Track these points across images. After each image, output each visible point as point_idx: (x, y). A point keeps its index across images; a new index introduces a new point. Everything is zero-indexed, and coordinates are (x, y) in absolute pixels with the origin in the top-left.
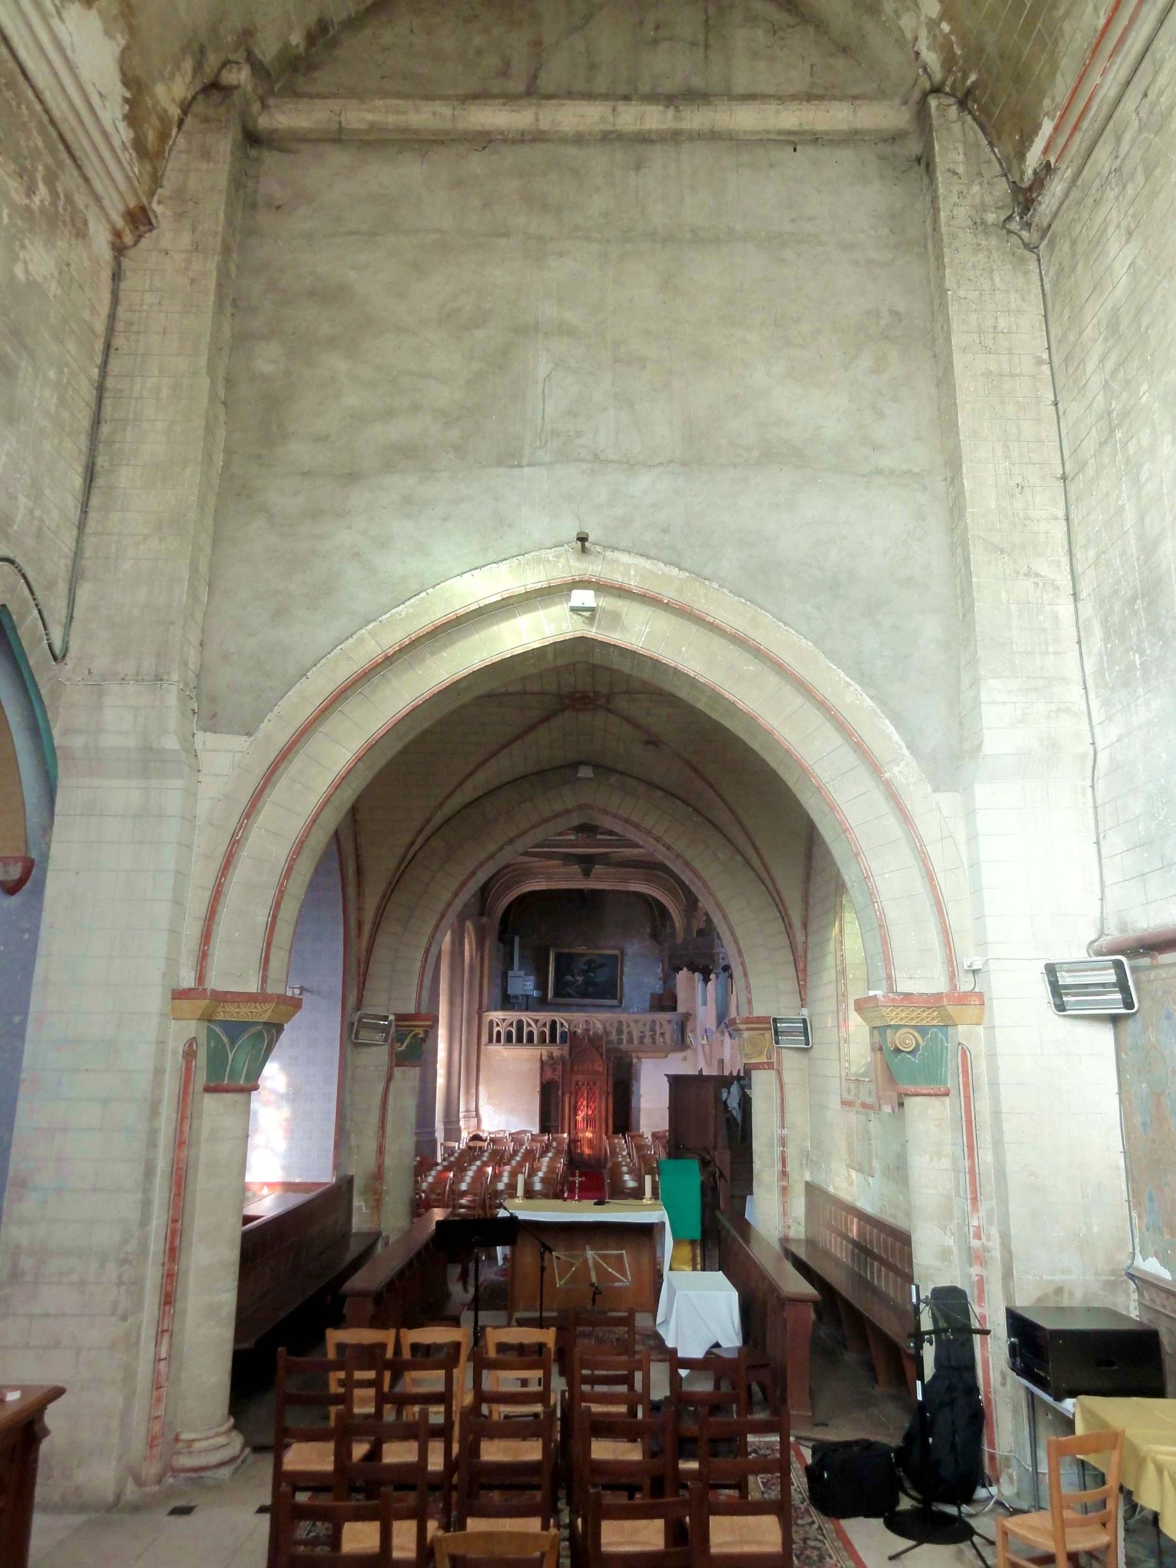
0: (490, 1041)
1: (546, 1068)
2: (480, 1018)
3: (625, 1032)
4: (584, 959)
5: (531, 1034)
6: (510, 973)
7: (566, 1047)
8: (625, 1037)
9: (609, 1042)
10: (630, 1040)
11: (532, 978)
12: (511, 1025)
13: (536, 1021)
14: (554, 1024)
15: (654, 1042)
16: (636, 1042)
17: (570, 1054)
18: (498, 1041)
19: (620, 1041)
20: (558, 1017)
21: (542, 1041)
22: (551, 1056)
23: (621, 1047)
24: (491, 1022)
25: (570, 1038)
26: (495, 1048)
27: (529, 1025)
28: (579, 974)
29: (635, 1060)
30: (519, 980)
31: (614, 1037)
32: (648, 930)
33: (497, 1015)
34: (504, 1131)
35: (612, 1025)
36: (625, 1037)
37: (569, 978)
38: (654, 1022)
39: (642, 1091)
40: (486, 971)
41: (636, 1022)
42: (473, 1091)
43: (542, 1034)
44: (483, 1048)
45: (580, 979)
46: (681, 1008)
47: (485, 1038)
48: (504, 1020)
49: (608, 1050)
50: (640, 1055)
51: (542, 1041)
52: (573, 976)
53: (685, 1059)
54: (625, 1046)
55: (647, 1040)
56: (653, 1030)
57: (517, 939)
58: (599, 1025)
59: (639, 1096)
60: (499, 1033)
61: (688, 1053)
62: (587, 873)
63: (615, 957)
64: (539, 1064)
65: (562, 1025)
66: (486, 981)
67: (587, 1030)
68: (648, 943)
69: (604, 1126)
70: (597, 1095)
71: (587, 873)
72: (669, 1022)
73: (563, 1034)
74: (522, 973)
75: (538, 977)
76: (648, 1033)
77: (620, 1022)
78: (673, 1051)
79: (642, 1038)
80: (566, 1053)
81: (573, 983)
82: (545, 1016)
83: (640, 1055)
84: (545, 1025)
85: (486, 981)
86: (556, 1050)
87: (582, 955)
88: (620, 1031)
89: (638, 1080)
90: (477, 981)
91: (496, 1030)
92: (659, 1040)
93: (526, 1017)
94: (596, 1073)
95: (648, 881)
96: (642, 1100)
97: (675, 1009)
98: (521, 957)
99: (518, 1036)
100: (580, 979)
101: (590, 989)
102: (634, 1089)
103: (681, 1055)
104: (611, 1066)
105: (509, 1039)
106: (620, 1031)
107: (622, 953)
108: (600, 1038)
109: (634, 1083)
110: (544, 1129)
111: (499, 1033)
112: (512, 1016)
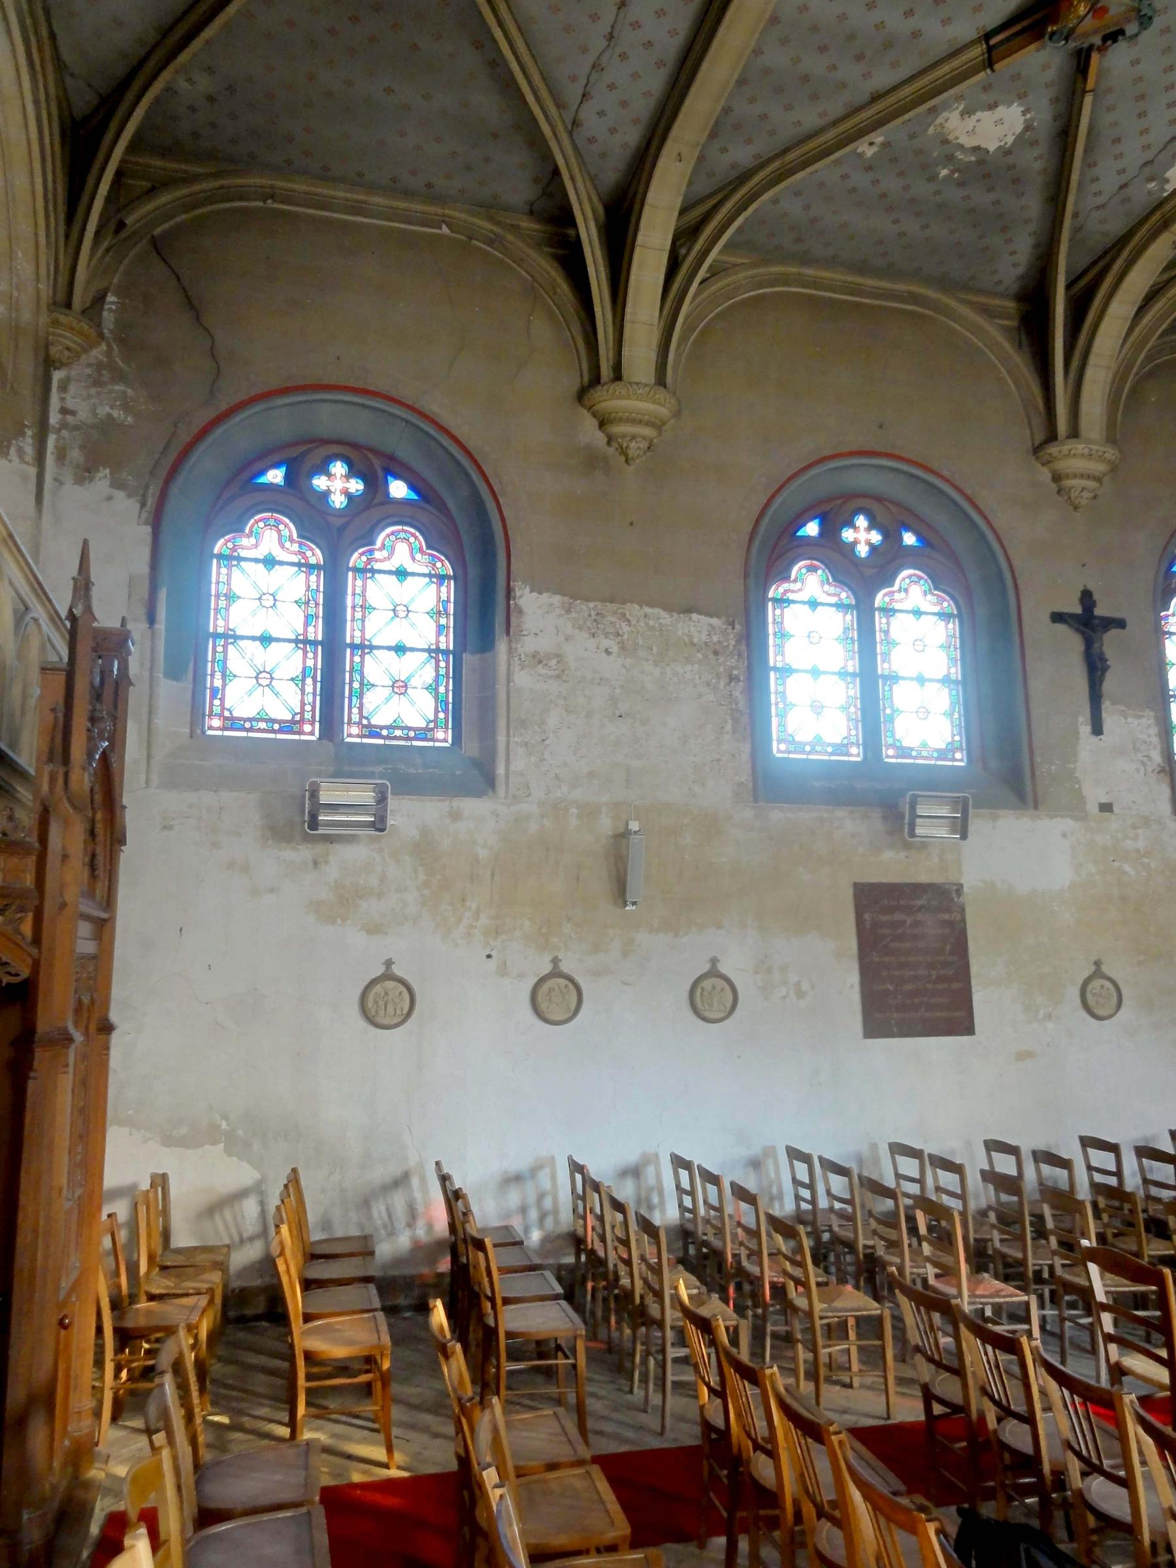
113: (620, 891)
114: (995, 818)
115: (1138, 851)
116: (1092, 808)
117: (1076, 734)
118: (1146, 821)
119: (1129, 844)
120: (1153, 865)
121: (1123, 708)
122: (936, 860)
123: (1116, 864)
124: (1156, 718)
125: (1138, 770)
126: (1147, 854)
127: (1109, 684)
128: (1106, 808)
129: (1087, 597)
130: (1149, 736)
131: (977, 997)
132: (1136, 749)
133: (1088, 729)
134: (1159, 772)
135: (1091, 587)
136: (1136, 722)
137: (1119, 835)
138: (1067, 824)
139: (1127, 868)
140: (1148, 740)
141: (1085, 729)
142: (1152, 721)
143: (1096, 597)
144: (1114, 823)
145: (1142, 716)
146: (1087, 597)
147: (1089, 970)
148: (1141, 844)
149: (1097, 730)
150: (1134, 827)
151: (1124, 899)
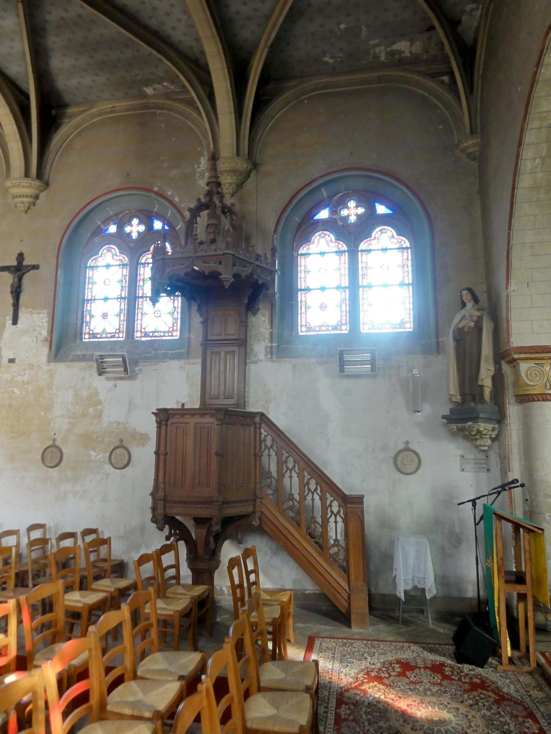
115: (23, 382)
116: (5, 361)
117: (4, 326)
118: (31, 366)
119: (19, 379)
120: (30, 388)
121: (31, 310)
123: (11, 388)
124: (48, 313)
125: (33, 341)
126: (28, 383)
127: (23, 298)
128: (12, 361)
129: (21, 257)
130: (43, 323)
132: (34, 330)
133: (11, 322)
134: (44, 341)
135: (23, 252)
136: (37, 316)
137: (16, 374)
139: (16, 391)
140: (41, 325)
141: (9, 322)
142: (46, 315)
143: (25, 256)
144: (14, 367)
145: (41, 313)
146: (21, 257)
150: (24, 370)
151: (10, 406)
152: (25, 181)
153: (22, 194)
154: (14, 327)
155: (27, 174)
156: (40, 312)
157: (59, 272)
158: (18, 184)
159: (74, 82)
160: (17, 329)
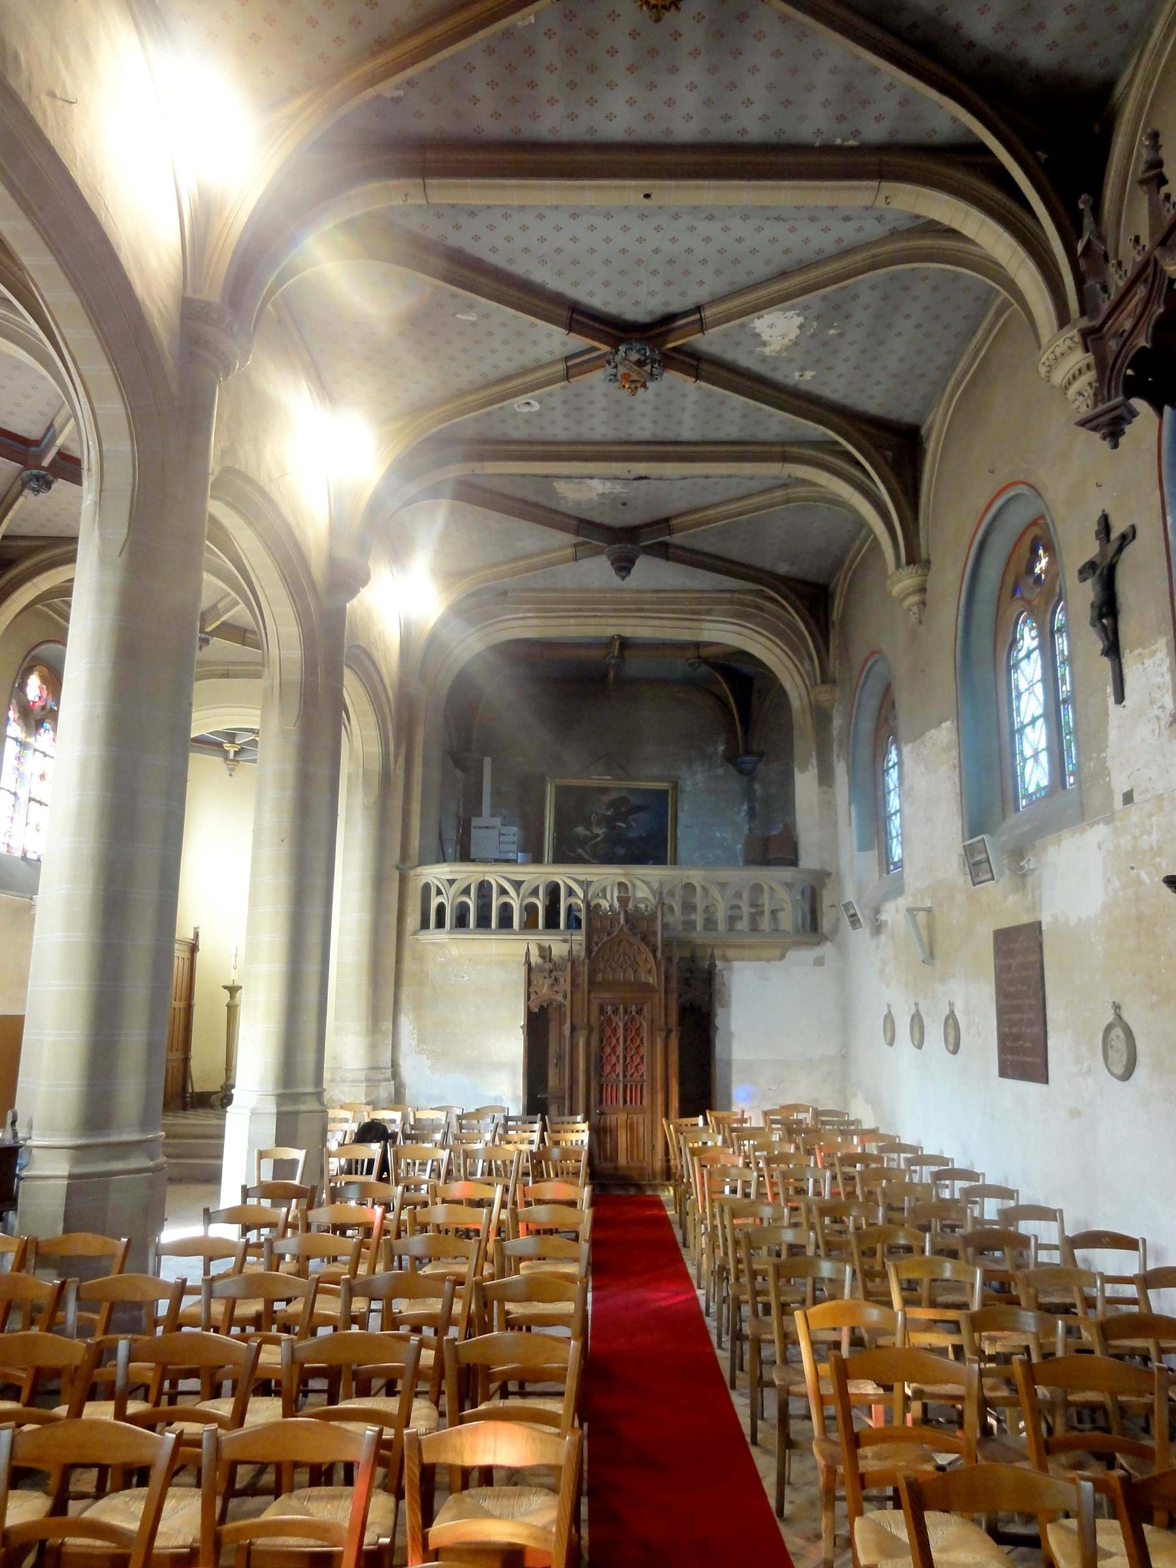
0: (425, 925)
1: (537, 979)
2: (403, 880)
3: (700, 907)
4: (607, 798)
5: (506, 909)
6: (475, 821)
7: (579, 937)
8: (698, 918)
9: (665, 926)
10: (710, 923)
11: (515, 829)
12: (466, 891)
13: (517, 885)
14: (553, 891)
15: (754, 928)
16: (722, 926)
17: (589, 950)
18: (440, 924)
19: (689, 925)
20: (564, 875)
21: (530, 923)
22: (545, 953)
23: (693, 935)
24: (426, 888)
25: (592, 921)
26: (434, 936)
27: (503, 892)
28: (598, 824)
29: (719, 964)
30: (493, 833)
31: (677, 917)
32: (721, 748)
33: (437, 873)
34: (447, 1109)
35: (671, 894)
36: (698, 918)
37: (580, 830)
38: (757, 889)
39: (735, 1027)
40: (417, 789)
41: (723, 886)
42: (387, 1026)
43: (531, 910)
44: (408, 938)
45: (600, 831)
46: (809, 859)
47: (413, 919)
48: (451, 882)
49: (667, 944)
50: (730, 953)
51: (530, 923)
52: (588, 829)
53: (819, 962)
54: (699, 935)
55: (743, 925)
56: (753, 904)
57: (487, 761)
58: (642, 892)
59: (730, 1035)
60: (441, 908)
61: (827, 949)
62: (623, 566)
63: (663, 794)
64: (522, 973)
65: (571, 892)
66: (416, 806)
67: (623, 901)
68: (720, 771)
69: (660, 1097)
70: (645, 1034)
71: (623, 566)
72: (789, 886)
73: (570, 909)
74: (497, 821)
75: (525, 828)
76: (746, 910)
77: (689, 887)
78: (797, 944)
79: (732, 920)
80: (580, 950)
81: (587, 839)
82: (537, 875)
83: (730, 953)
84: (535, 892)
85: (416, 806)
86: (560, 945)
87: (604, 790)
88: (688, 907)
89: (726, 1005)
90: (397, 803)
91: (435, 902)
92: (765, 923)
93: (495, 875)
94: (647, 987)
95: (743, 613)
96: (735, 1045)
97: (794, 862)
98: (496, 793)
99: (482, 914)
100: (600, 831)
101: (620, 851)
102: (719, 1022)
103: (809, 954)
104: (674, 971)
105: (461, 922)
106: (688, 907)
107: (675, 786)
108: (652, 918)
109: (720, 1012)
110: (537, 1103)
111: (441, 908)
112: (469, 874)
113: (930, 955)
114: (1059, 840)
115: (1151, 848)
119: (1146, 841)
121: (1139, 650)
122: (1030, 898)
123: (1135, 871)
125: (1153, 731)
129: (1105, 525)
131: (1051, 1043)
132: (1152, 703)
138: (1099, 832)
142: (1165, 651)
144: (1135, 815)
147: (1110, 1017)
148: (1154, 838)
149: (1120, 697)
150: (1150, 816)
151: (1140, 918)
152: (1060, 342)
153: (1070, 375)
154: (1119, 707)
155: (1063, 319)
156: (1154, 648)
157: (1169, 519)
158: (1052, 357)
159: (1058, 23)
160: (1126, 711)
